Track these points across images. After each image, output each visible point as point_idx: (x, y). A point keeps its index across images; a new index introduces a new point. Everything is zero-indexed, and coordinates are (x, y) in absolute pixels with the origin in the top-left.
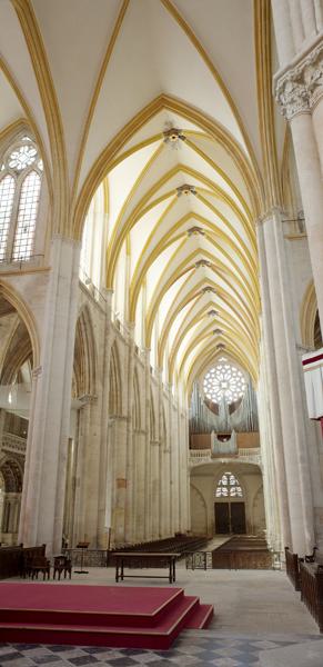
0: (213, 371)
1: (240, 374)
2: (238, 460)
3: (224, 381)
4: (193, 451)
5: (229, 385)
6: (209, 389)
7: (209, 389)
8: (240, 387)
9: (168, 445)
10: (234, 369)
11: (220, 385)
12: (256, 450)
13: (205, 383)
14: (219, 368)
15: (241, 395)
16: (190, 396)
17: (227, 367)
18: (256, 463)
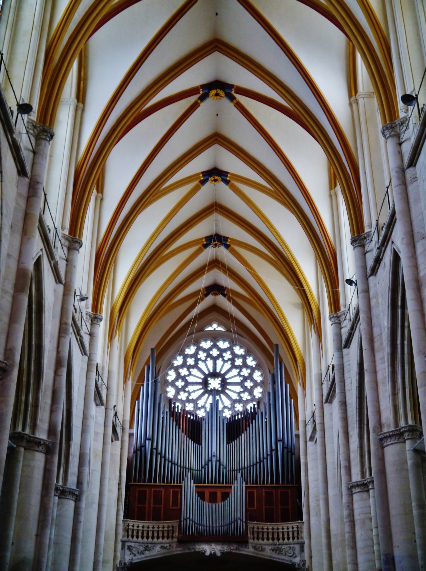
0: (191, 350)
1: (250, 362)
2: (249, 551)
3: (214, 375)
4: (131, 522)
5: (224, 384)
6: (178, 391)
7: (178, 391)
8: (251, 391)
9: (72, 480)
10: (239, 351)
11: (205, 383)
12: (292, 525)
13: (172, 376)
14: (206, 345)
15: (250, 406)
16: (136, 396)
17: (223, 345)
18: (284, 558)
